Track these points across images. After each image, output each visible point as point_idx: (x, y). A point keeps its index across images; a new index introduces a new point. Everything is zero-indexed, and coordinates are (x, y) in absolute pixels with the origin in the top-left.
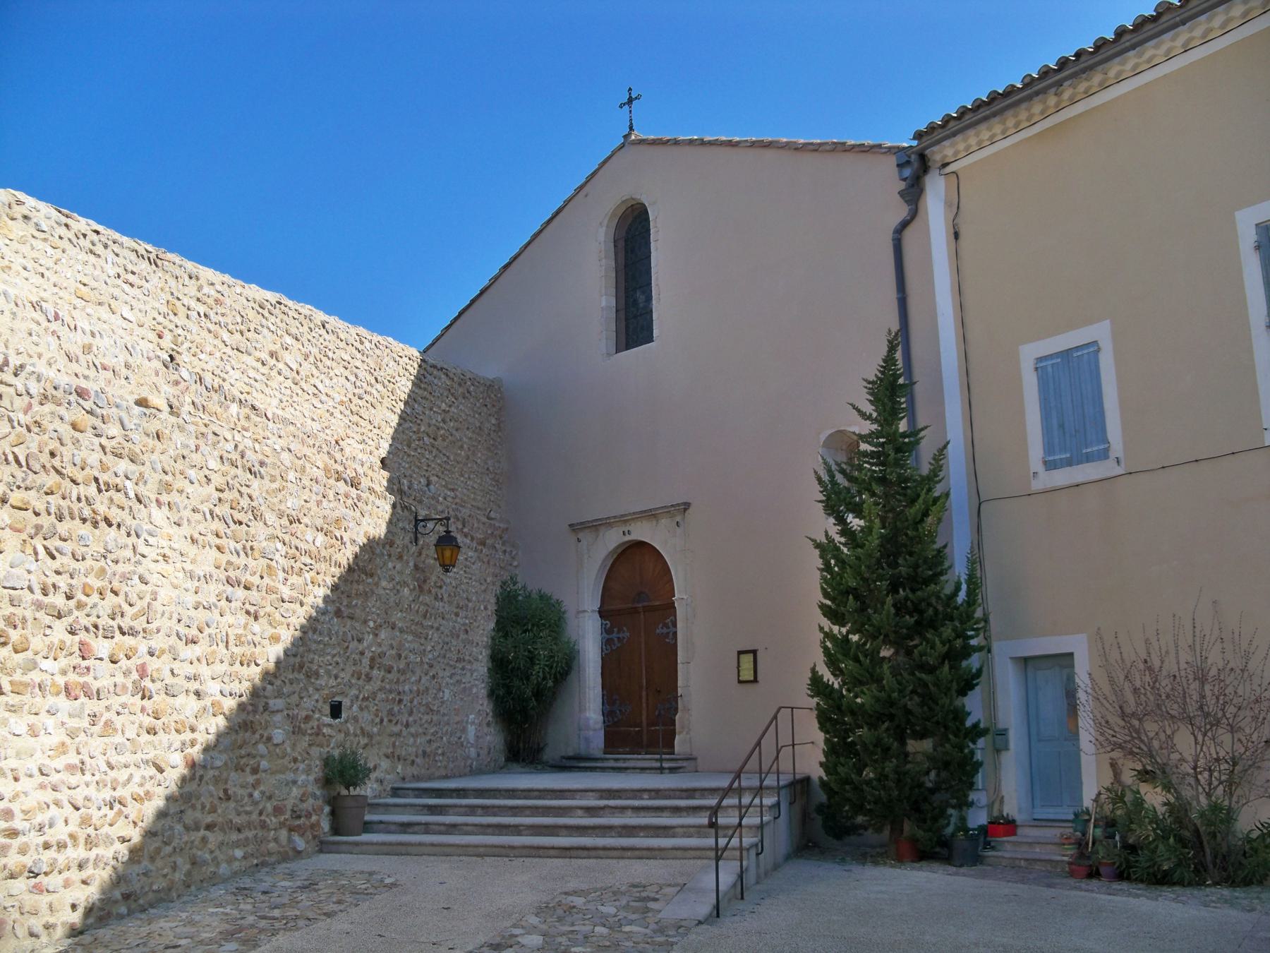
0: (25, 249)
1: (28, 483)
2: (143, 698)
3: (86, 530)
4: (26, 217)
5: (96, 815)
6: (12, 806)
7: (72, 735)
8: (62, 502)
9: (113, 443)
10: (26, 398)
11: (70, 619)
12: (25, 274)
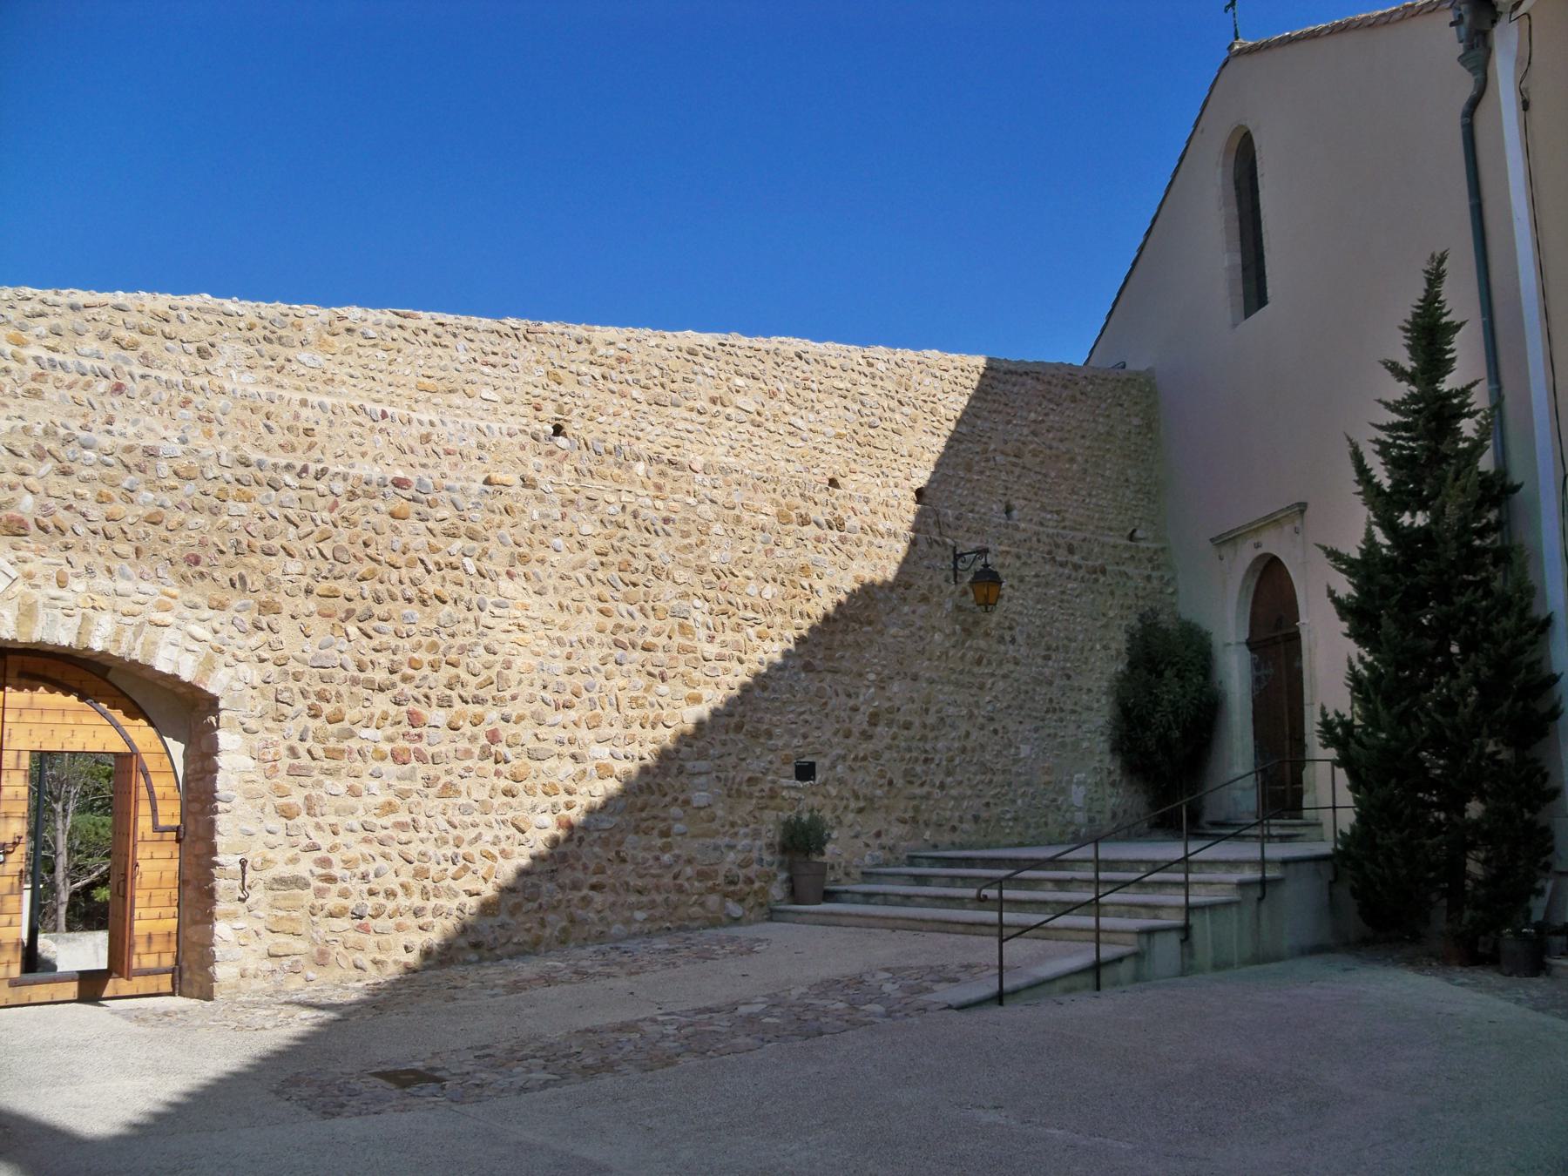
0: (348, 359)
1: (336, 573)
2: (497, 762)
3: (414, 610)
4: (349, 330)
5: (434, 870)
6: (330, 856)
7: (403, 795)
8: (379, 586)
9: (445, 524)
10: (332, 498)
11: (396, 692)
12: (353, 381)
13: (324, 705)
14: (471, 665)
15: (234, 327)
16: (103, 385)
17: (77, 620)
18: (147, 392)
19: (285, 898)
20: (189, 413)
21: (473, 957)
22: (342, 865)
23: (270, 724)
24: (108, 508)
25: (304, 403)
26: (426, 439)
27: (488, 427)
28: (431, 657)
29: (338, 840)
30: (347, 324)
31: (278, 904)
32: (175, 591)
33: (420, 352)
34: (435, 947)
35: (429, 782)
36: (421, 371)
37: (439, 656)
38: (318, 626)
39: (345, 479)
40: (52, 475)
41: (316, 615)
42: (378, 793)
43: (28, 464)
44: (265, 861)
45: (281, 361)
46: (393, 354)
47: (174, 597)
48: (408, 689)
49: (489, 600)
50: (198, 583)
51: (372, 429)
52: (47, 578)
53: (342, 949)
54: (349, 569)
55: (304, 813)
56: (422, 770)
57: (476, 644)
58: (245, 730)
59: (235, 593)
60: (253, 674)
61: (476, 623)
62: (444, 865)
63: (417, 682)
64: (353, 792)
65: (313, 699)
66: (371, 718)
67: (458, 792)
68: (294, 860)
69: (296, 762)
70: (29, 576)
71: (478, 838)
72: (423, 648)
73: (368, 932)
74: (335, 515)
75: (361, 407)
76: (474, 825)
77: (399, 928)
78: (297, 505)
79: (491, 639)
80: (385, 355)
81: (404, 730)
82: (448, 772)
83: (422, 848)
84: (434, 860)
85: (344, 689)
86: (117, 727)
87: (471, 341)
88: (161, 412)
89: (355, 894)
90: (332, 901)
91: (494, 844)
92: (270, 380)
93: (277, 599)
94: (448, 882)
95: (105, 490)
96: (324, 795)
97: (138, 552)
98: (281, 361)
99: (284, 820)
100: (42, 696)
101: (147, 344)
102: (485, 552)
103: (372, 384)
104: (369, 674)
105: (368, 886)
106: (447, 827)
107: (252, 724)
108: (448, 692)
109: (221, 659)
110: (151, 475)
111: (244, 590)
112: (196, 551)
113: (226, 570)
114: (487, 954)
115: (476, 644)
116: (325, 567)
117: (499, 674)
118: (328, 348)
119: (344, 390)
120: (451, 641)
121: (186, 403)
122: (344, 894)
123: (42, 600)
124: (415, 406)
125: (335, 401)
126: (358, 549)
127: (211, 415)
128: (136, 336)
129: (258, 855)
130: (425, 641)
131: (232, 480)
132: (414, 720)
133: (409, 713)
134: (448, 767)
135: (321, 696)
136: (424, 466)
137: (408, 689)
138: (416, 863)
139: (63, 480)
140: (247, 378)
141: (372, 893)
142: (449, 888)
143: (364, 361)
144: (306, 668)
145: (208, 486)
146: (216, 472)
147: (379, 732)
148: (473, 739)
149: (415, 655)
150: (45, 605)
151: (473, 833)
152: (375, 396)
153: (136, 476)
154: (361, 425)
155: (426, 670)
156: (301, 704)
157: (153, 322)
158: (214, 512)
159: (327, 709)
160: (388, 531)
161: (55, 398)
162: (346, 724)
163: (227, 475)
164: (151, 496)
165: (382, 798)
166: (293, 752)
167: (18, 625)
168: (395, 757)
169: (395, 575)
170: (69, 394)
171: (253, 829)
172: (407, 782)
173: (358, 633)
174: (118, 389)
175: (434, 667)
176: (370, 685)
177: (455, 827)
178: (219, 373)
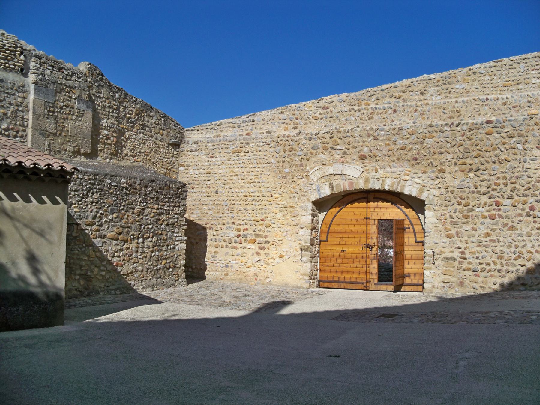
0: (475, 83)
1: (465, 157)
2: (534, 218)
3: (497, 166)
4: (474, 73)
5: (506, 257)
6: (465, 251)
7: (493, 230)
8: (482, 159)
9: (508, 133)
10: (463, 132)
11: (489, 195)
12: (477, 90)
13: (462, 201)
14: (521, 183)
15: (432, 83)
16: (390, 111)
17: (381, 181)
18: (404, 110)
19: (448, 264)
20: (418, 113)
21: (522, 288)
22: (469, 254)
23: (443, 208)
24: (389, 147)
25: (457, 102)
26: (505, 104)
27: (532, 94)
28: (504, 181)
29: (468, 245)
30: (473, 71)
31: (445, 266)
32: (410, 169)
33: (504, 73)
34: (505, 284)
35: (504, 225)
36: (505, 80)
37: (507, 181)
38: (459, 175)
39: (467, 125)
40: (372, 141)
41: (459, 171)
42: (484, 229)
43: (366, 139)
44: (441, 252)
45: (450, 89)
46: (492, 77)
47: (410, 171)
48: (495, 193)
49: (528, 158)
50: (418, 166)
51: (483, 105)
52: (372, 170)
53: (468, 282)
54: (470, 155)
55: (456, 236)
56: (501, 221)
57: (522, 175)
58: (434, 210)
59: (430, 168)
60: (436, 192)
61: (523, 167)
62: (510, 255)
63: (498, 190)
64: (474, 229)
65: (459, 199)
66: (480, 204)
67: (517, 229)
68: (452, 252)
69: (453, 220)
70: (367, 170)
71: (525, 246)
72: (501, 179)
73: (478, 276)
74: (464, 137)
75: (478, 98)
76: (524, 241)
77: (492, 276)
78: (450, 136)
79: (530, 172)
80: (489, 78)
81: (494, 208)
82: (513, 222)
83: (501, 249)
84: (506, 253)
85: (469, 195)
86: (403, 211)
87: (526, 63)
88: (408, 115)
89: (474, 264)
90: (465, 265)
91: (532, 248)
92: (446, 97)
93: (444, 168)
94: (512, 261)
95: (387, 142)
96: (463, 231)
97: (398, 159)
98: (450, 89)
99: (449, 239)
100: (381, 204)
101: (404, 95)
102: (526, 141)
103: (484, 89)
104: (479, 189)
105: (479, 261)
106: (512, 241)
107: (437, 208)
108: (511, 193)
109: (426, 189)
110: (401, 135)
111: (433, 166)
112: (416, 156)
113: (427, 161)
114: (529, 288)
115: (522, 175)
116: (461, 155)
117: (533, 185)
118: (466, 81)
119: (474, 94)
120: (512, 175)
121: (416, 111)
122: (470, 263)
123: (371, 177)
124: (502, 93)
125: (468, 98)
126: (474, 148)
127: (425, 113)
128: (401, 94)
129: (439, 250)
130: (501, 176)
131: (427, 132)
132: (498, 204)
133: (496, 202)
134: (512, 220)
135: (461, 198)
136: (504, 114)
137: (495, 193)
138: (499, 254)
139: (375, 142)
140: (439, 98)
141: (480, 264)
142: (512, 263)
143: (481, 82)
144: (455, 189)
145: (419, 136)
146: (421, 130)
147: (483, 209)
148: (523, 210)
149: (497, 181)
150: (372, 178)
151: (523, 243)
152: (486, 93)
153: (397, 136)
154: (478, 104)
155: (502, 186)
156: (454, 201)
157: (405, 88)
158: (422, 143)
159: (463, 202)
160: (485, 139)
161: (377, 118)
162: (471, 207)
163: (425, 131)
164: (402, 141)
165: (485, 231)
166: (451, 217)
167: (364, 184)
168: (492, 217)
169: (488, 154)
170: (380, 116)
171: (437, 242)
172: (496, 226)
173: (475, 176)
174: (395, 111)
175: (506, 185)
176: (479, 193)
177: (515, 242)
178: (428, 98)
